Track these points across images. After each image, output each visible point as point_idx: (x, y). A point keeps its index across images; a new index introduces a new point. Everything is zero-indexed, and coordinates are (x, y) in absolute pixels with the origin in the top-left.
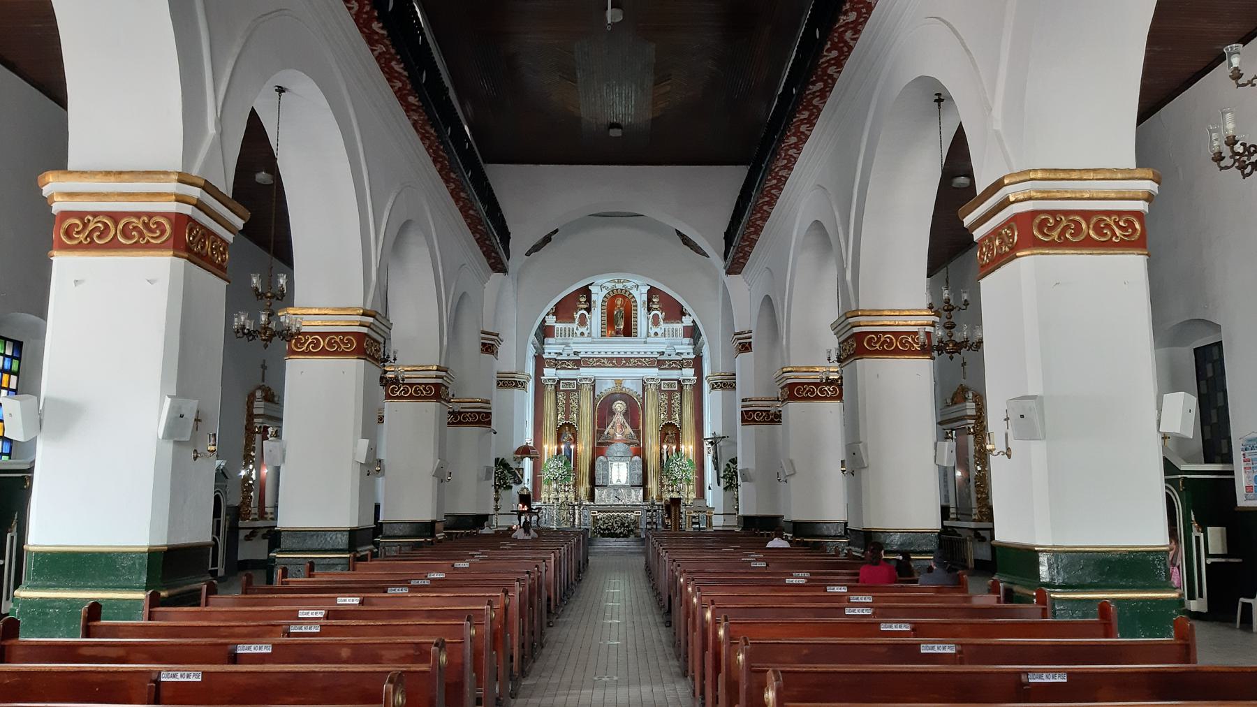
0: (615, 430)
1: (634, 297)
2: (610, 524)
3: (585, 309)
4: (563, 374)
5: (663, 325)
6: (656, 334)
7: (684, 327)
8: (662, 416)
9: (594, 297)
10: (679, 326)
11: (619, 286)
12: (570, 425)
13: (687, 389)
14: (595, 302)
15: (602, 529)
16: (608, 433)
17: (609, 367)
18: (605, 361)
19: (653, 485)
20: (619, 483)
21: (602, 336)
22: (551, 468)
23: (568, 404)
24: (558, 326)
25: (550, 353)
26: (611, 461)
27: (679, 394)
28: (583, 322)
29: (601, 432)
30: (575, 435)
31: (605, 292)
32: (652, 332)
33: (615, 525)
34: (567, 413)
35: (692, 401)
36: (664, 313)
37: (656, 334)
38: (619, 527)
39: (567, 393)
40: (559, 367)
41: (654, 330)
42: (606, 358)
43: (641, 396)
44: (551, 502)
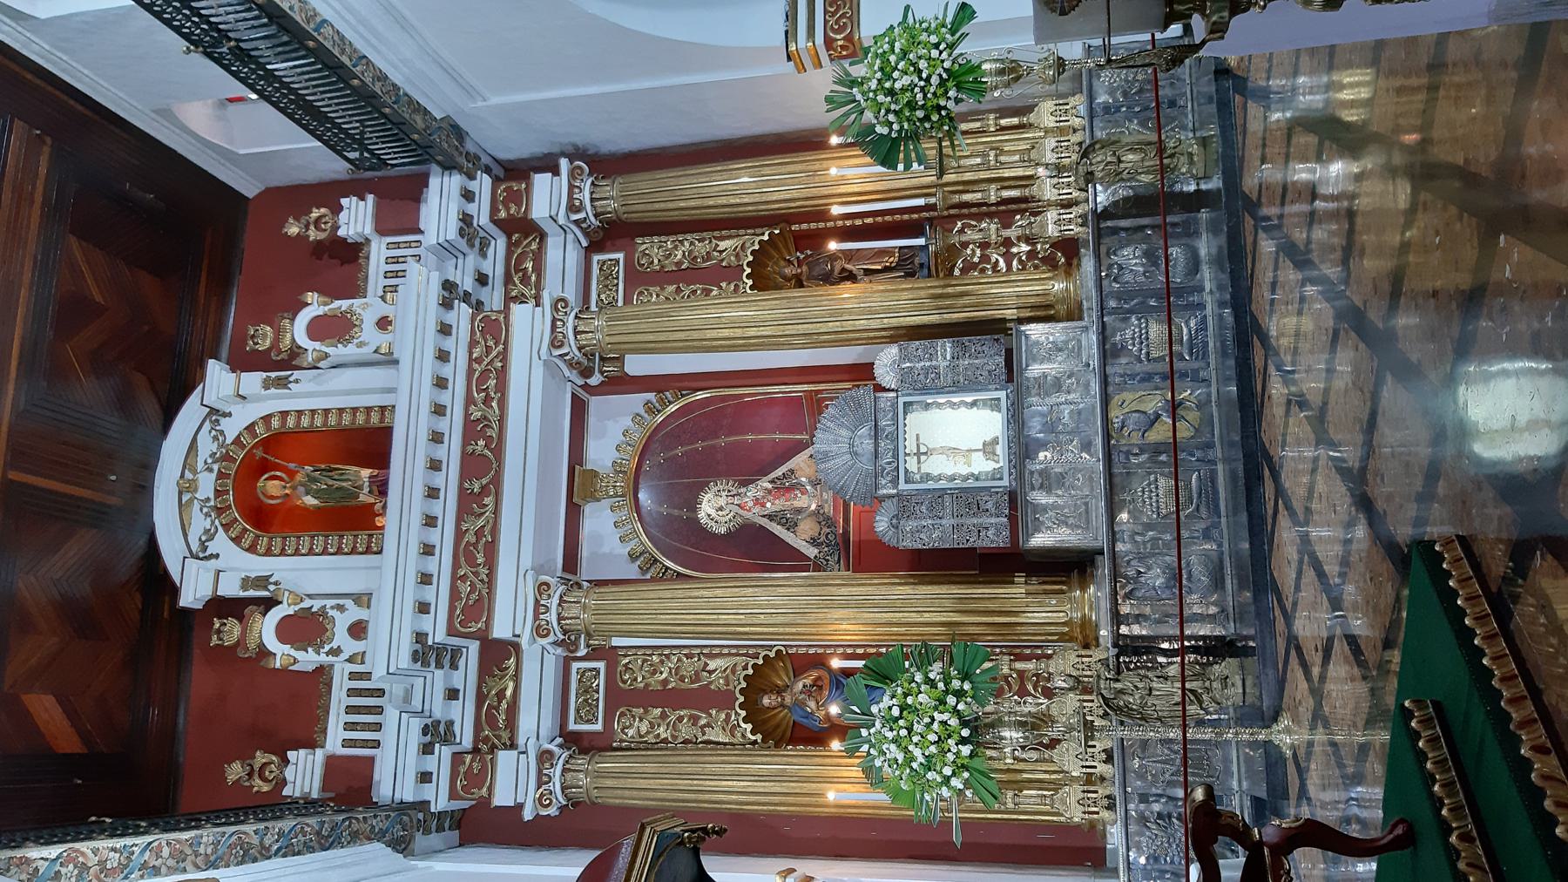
1: (250, 428)
7: (381, 230)
10: (379, 252)
11: (206, 485)
12: (758, 683)
13: (615, 197)
14: (246, 583)
16: (814, 542)
20: (1000, 449)
23: (668, 698)
24: (335, 739)
25: (425, 777)
26: (895, 481)
27: (644, 244)
31: (221, 543)
34: (704, 699)
37: (383, 323)
39: (621, 698)
40: (505, 735)
41: (369, 334)
42: (459, 520)
43: (651, 396)
44: (1102, 769)
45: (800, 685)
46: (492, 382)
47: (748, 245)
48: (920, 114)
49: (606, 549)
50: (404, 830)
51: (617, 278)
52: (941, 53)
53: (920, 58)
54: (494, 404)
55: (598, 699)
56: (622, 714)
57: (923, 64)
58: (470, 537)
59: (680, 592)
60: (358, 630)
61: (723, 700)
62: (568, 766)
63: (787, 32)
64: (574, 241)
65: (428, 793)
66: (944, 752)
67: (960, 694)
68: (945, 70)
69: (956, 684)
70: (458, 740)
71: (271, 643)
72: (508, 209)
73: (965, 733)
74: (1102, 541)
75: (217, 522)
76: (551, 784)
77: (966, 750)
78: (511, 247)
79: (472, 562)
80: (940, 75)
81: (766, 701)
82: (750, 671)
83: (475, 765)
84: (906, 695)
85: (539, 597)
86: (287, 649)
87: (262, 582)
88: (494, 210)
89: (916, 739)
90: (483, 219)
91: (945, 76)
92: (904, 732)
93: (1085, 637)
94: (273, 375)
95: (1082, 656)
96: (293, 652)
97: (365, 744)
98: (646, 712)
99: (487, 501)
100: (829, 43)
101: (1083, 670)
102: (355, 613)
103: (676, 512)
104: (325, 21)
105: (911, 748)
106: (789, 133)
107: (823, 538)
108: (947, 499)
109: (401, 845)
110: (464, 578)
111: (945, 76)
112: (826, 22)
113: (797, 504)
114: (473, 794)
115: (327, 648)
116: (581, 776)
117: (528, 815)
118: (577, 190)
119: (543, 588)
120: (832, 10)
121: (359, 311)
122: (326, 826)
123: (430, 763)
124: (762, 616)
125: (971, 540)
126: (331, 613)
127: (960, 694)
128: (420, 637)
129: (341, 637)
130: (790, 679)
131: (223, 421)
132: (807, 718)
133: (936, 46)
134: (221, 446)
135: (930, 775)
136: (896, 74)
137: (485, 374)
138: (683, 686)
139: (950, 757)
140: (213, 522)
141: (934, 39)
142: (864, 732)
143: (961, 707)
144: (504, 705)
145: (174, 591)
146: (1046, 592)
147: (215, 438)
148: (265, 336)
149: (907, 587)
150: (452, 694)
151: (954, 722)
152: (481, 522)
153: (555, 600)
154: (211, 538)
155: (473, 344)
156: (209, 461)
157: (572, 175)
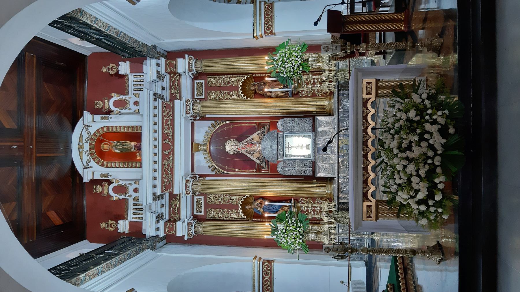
0: (255, 151)
1: (98, 130)
2: (411, 168)
3: (109, 185)
4: (185, 212)
5: (131, 98)
6: (136, 103)
7: (131, 72)
8: (235, 97)
9: (97, 176)
10: (131, 78)
11: (87, 147)
12: (245, 203)
13: (202, 66)
14: (102, 175)
15: (431, 195)
16: (258, 159)
17: (173, 160)
18: (166, 163)
19: (313, 105)
20: (310, 147)
21: (140, 167)
22: (287, 242)
23: (221, 207)
24: (130, 217)
25: (158, 229)
28: (121, 189)
29: (259, 168)
30: (257, 198)
31: (93, 163)
32: (134, 108)
33: (416, 152)
35: (215, 60)
36: (113, 95)
37: (136, 103)
38: (422, 139)
39: (208, 206)
40: (178, 216)
41: (131, 106)
42: (163, 162)
43: (213, 122)
45: (256, 204)
46: (169, 122)
47: (240, 80)
48: (292, 73)
49: (202, 165)
50: (154, 244)
51: (202, 88)
52: (298, 58)
53: (293, 60)
54: (171, 129)
55: (202, 206)
56: (209, 210)
57: (293, 62)
58: (166, 167)
59: (225, 183)
60: (136, 190)
61: (236, 207)
62: (196, 226)
63: (253, 30)
64: (190, 77)
65: (158, 233)
66: (296, 241)
67: (300, 227)
68: (299, 63)
69: (299, 224)
70: (165, 218)
71: (112, 193)
72: (170, 69)
73: (301, 237)
74: (336, 174)
75: (91, 157)
76: (192, 231)
77: (301, 241)
78: (171, 78)
79: (167, 174)
80: (298, 65)
81: (247, 207)
82: (243, 200)
83: (171, 225)
84: (287, 227)
85: (186, 184)
86: (116, 195)
87: (107, 175)
88: (166, 69)
89: (289, 238)
90: (163, 72)
91: (299, 65)
92: (286, 236)
93: (331, 198)
94: (104, 116)
95: (330, 204)
96: (118, 196)
97: (139, 218)
98: (215, 210)
99: (170, 156)
100: (265, 32)
101: (330, 207)
102: (135, 186)
103: (219, 148)
104: (121, 32)
105: (288, 239)
106: (253, 47)
107: (261, 158)
108: (296, 162)
109: (153, 248)
110: (165, 177)
111: (299, 65)
112: (265, 27)
113: (254, 148)
114: (171, 233)
115: (127, 195)
116: (199, 228)
117: (186, 238)
118: (191, 65)
119: (187, 181)
120: (266, 23)
121: (128, 99)
122: (137, 249)
123: (159, 225)
124: (247, 190)
125: (302, 173)
126: (128, 185)
127: (300, 227)
128: (154, 194)
129: (131, 192)
130: (253, 201)
131: (89, 128)
132: (258, 212)
133: (297, 57)
134: (89, 136)
135: (292, 246)
136: (286, 63)
137: (167, 120)
138: (225, 203)
139: (297, 242)
140: (90, 158)
141: (296, 54)
142: (276, 233)
143: (300, 231)
144: (177, 208)
145: (81, 178)
146: (321, 186)
147: (88, 133)
148: (100, 104)
149: (285, 184)
150: (163, 206)
151: (298, 234)
152: (169, 162)
153: (191, 184)
154: (90, 162)
155: (163, 111)
156: (87, 140)
157: (189, 59)
